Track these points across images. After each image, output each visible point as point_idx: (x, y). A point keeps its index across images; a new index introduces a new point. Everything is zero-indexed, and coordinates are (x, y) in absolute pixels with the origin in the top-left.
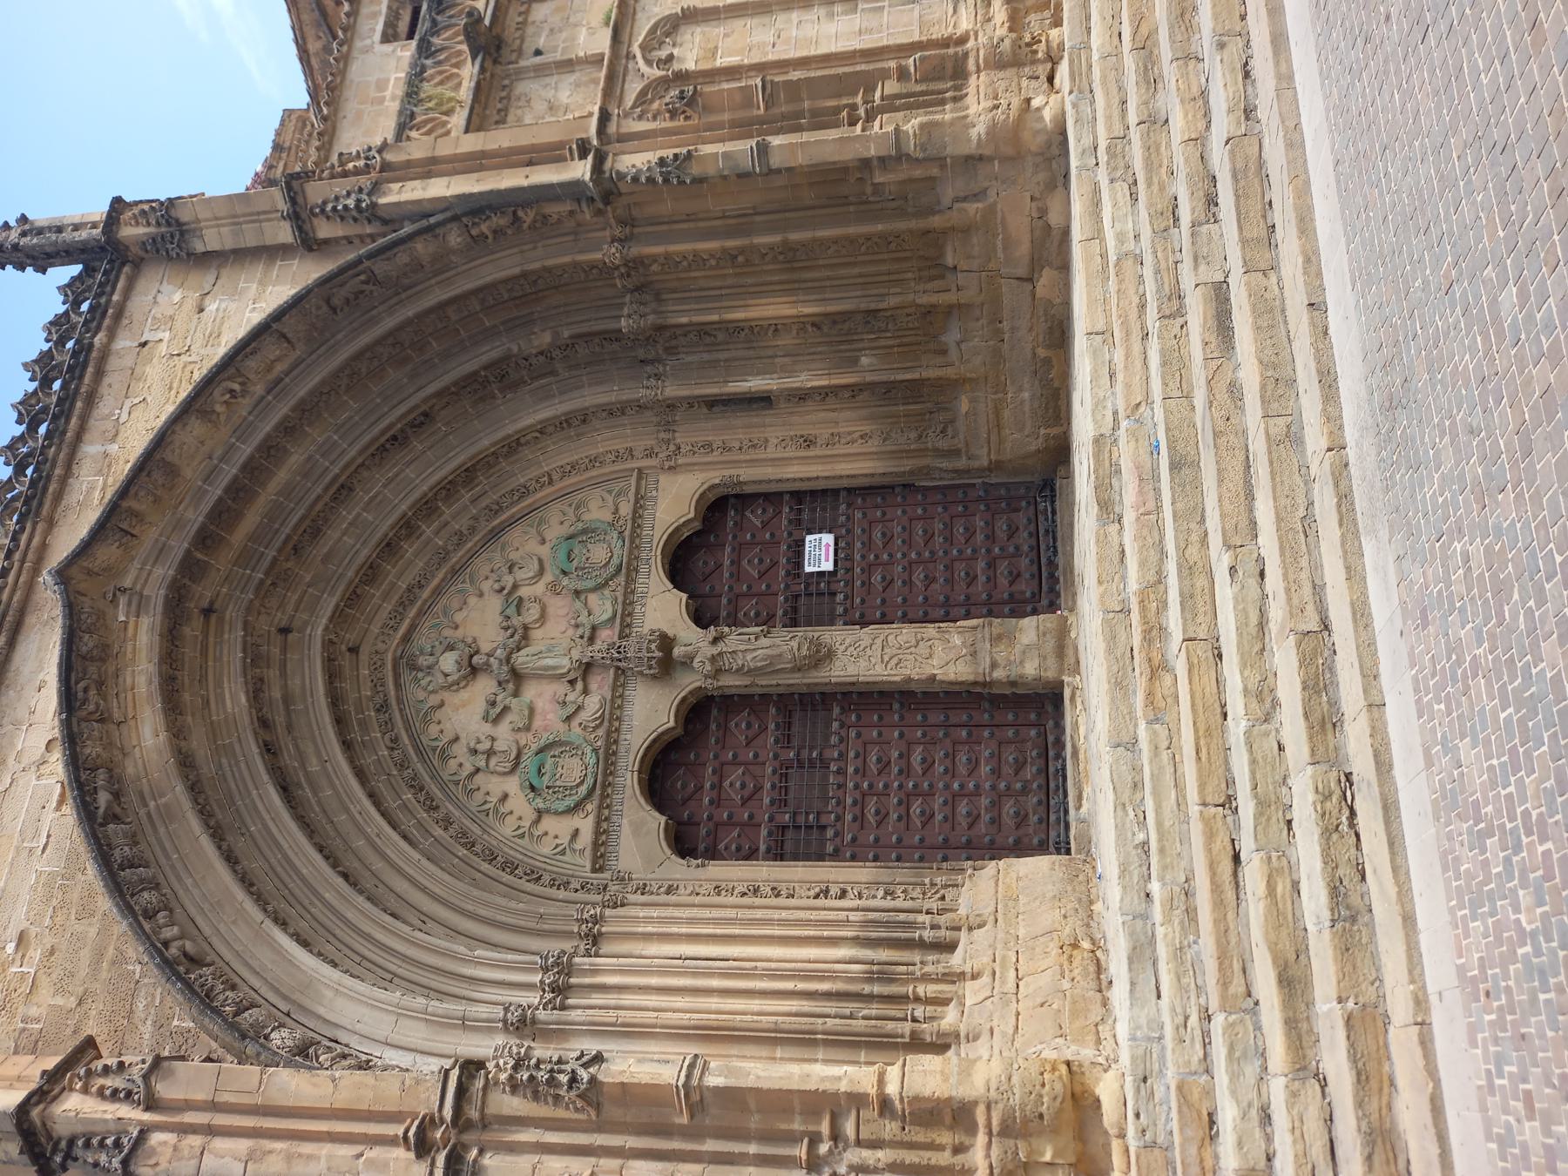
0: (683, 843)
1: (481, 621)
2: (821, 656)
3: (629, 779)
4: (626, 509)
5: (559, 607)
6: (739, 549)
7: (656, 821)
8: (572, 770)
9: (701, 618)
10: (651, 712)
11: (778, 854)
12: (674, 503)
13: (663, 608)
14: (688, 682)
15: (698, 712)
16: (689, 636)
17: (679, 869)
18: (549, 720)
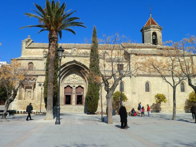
0: (65, 88)
1: (77, 76)
2: (74, 94)
3: (68, 85)
4: (83, 83)
5: (77, 80)
6: (81, 89)
7: (66, 86)
8: (69, 82)
9: (77, 88)
10: (71, 86)
11: (65, 92)
12: (82, 86)
13: (77, 86)
14: (73, 87)
15: (71, 88)
16: (75, 87)
17: (64, 88)
18: (71, 80)
